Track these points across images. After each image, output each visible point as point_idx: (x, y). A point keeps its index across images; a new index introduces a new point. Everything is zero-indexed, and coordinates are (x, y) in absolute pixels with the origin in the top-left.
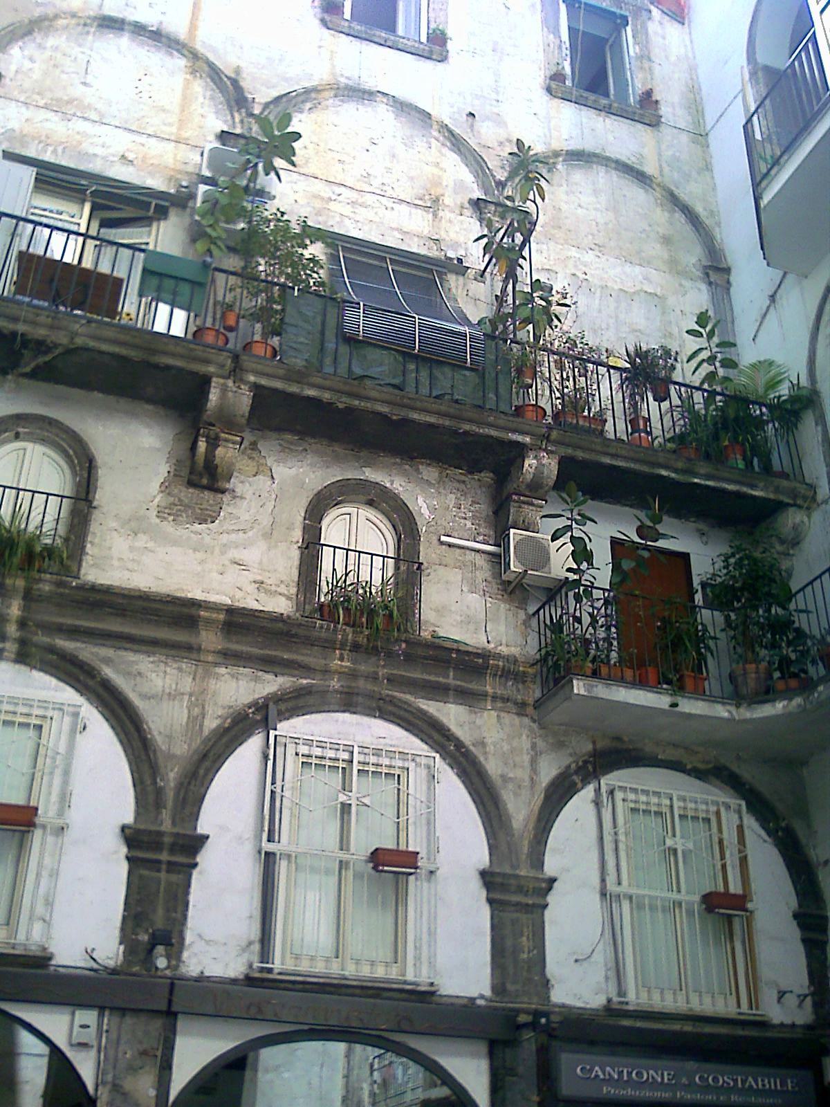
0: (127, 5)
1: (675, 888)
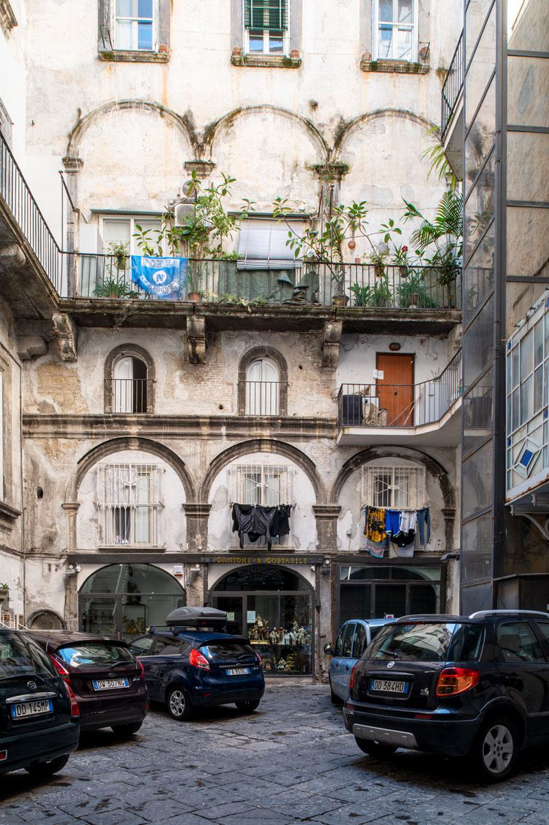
0: (131, 88)
1: (334, 515)
